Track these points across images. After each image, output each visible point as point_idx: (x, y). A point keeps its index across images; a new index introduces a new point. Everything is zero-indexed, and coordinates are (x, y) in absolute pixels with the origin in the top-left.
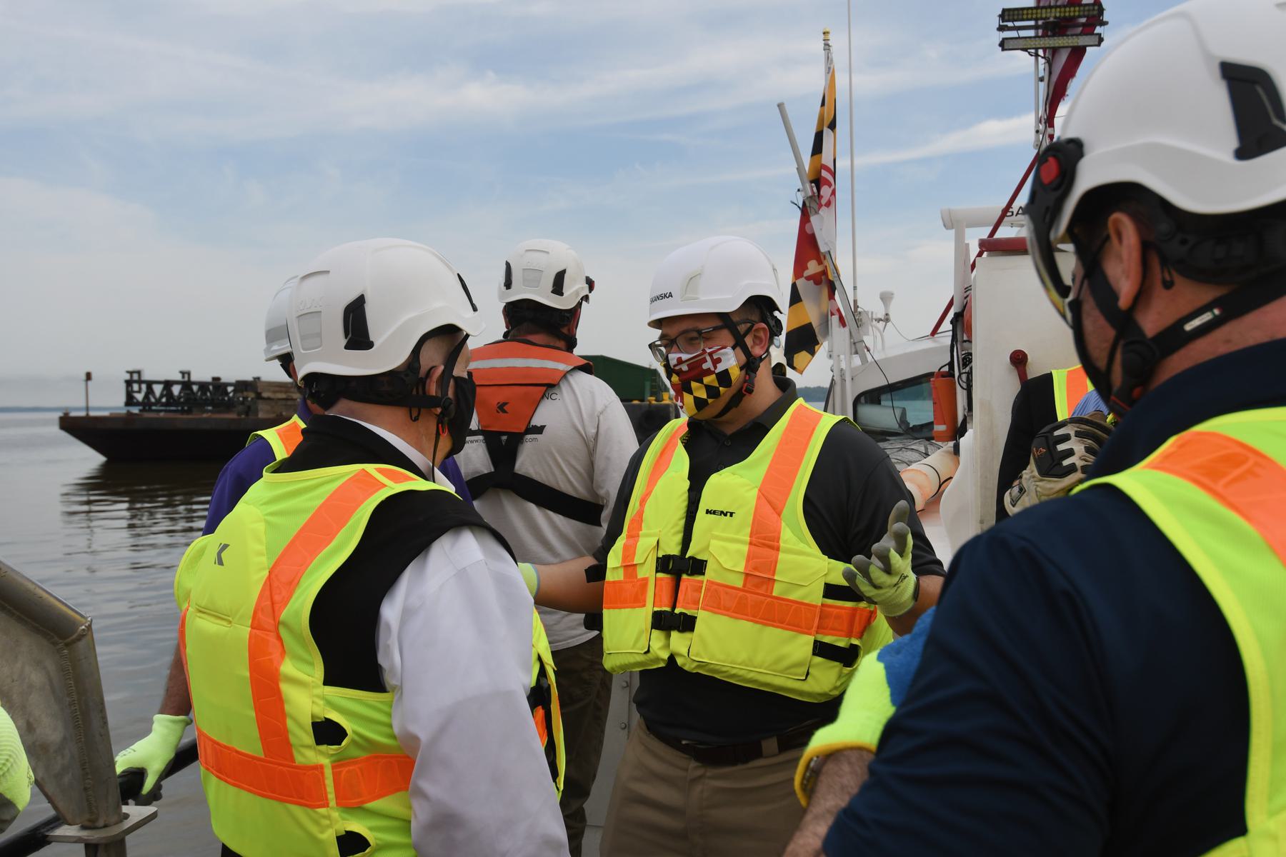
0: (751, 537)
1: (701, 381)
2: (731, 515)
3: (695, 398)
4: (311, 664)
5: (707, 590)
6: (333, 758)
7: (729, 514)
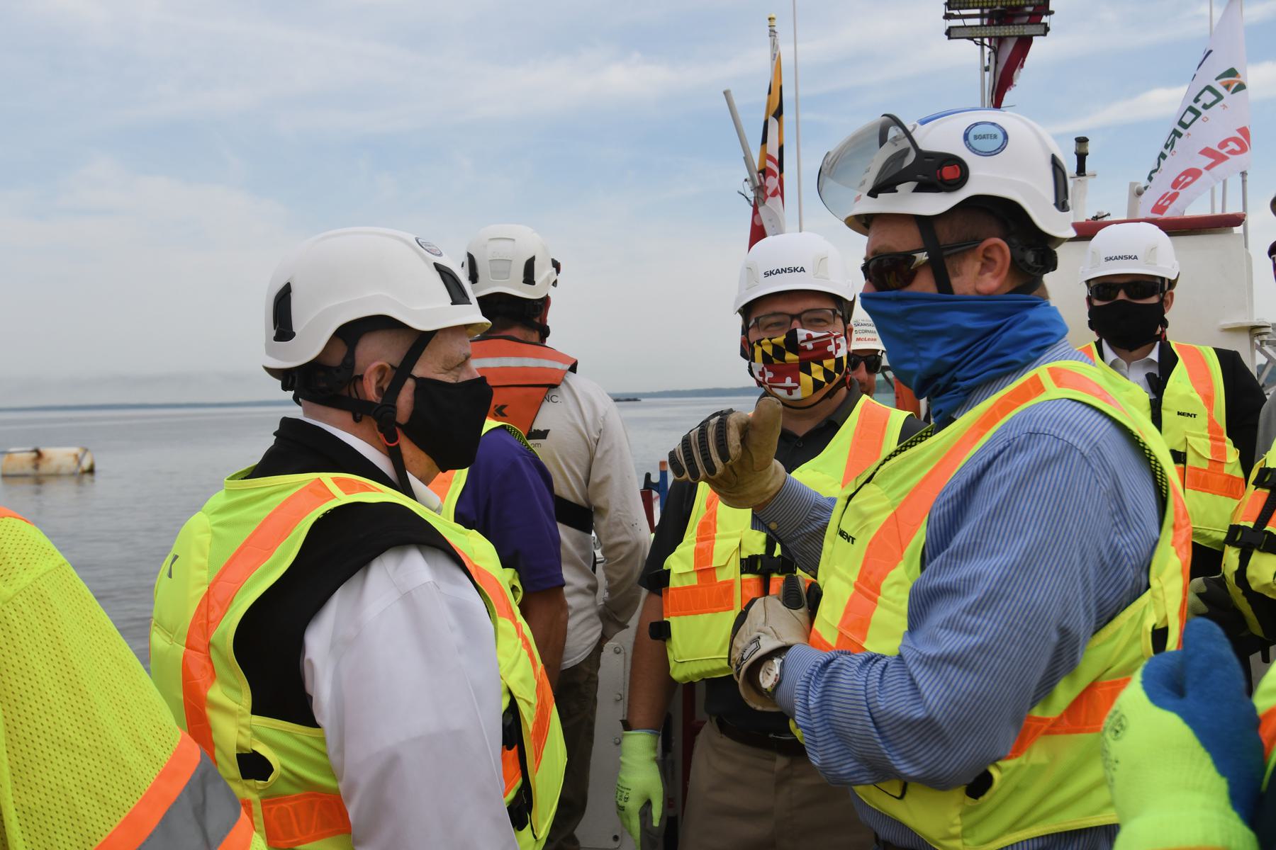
1: (822, 364)
3: (814, 379)
4: (239, 690)
6: (262, 794)
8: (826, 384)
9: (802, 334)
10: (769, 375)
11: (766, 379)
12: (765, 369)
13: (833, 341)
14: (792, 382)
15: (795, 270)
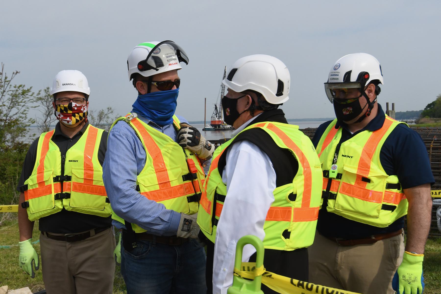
0: (84, 167)
2: (77, 161)
3: (76, 119)
5: (73, 185)
7: (76, 161)
8: (80, 121)
9: (74, 104)
10: (62, 116)
11: (61, 117)
12: (61, 114)
13: (83, 107)
14: (69, 119)
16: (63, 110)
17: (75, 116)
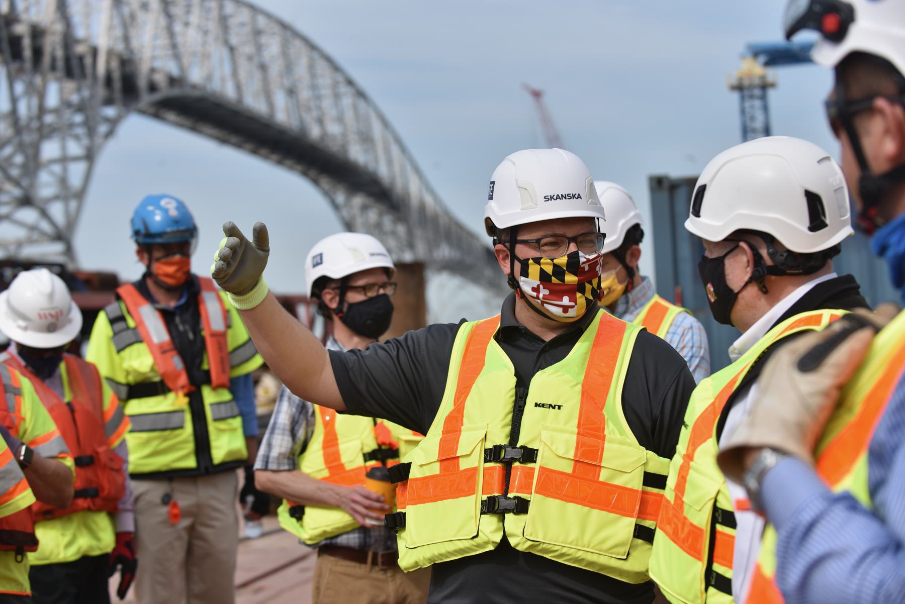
10: (544, 292)
11: (541, 296)
12: (541, 286)
14: (570, 301)
15: (574, 196)
16: (551, 274)
17: (583, 291)
